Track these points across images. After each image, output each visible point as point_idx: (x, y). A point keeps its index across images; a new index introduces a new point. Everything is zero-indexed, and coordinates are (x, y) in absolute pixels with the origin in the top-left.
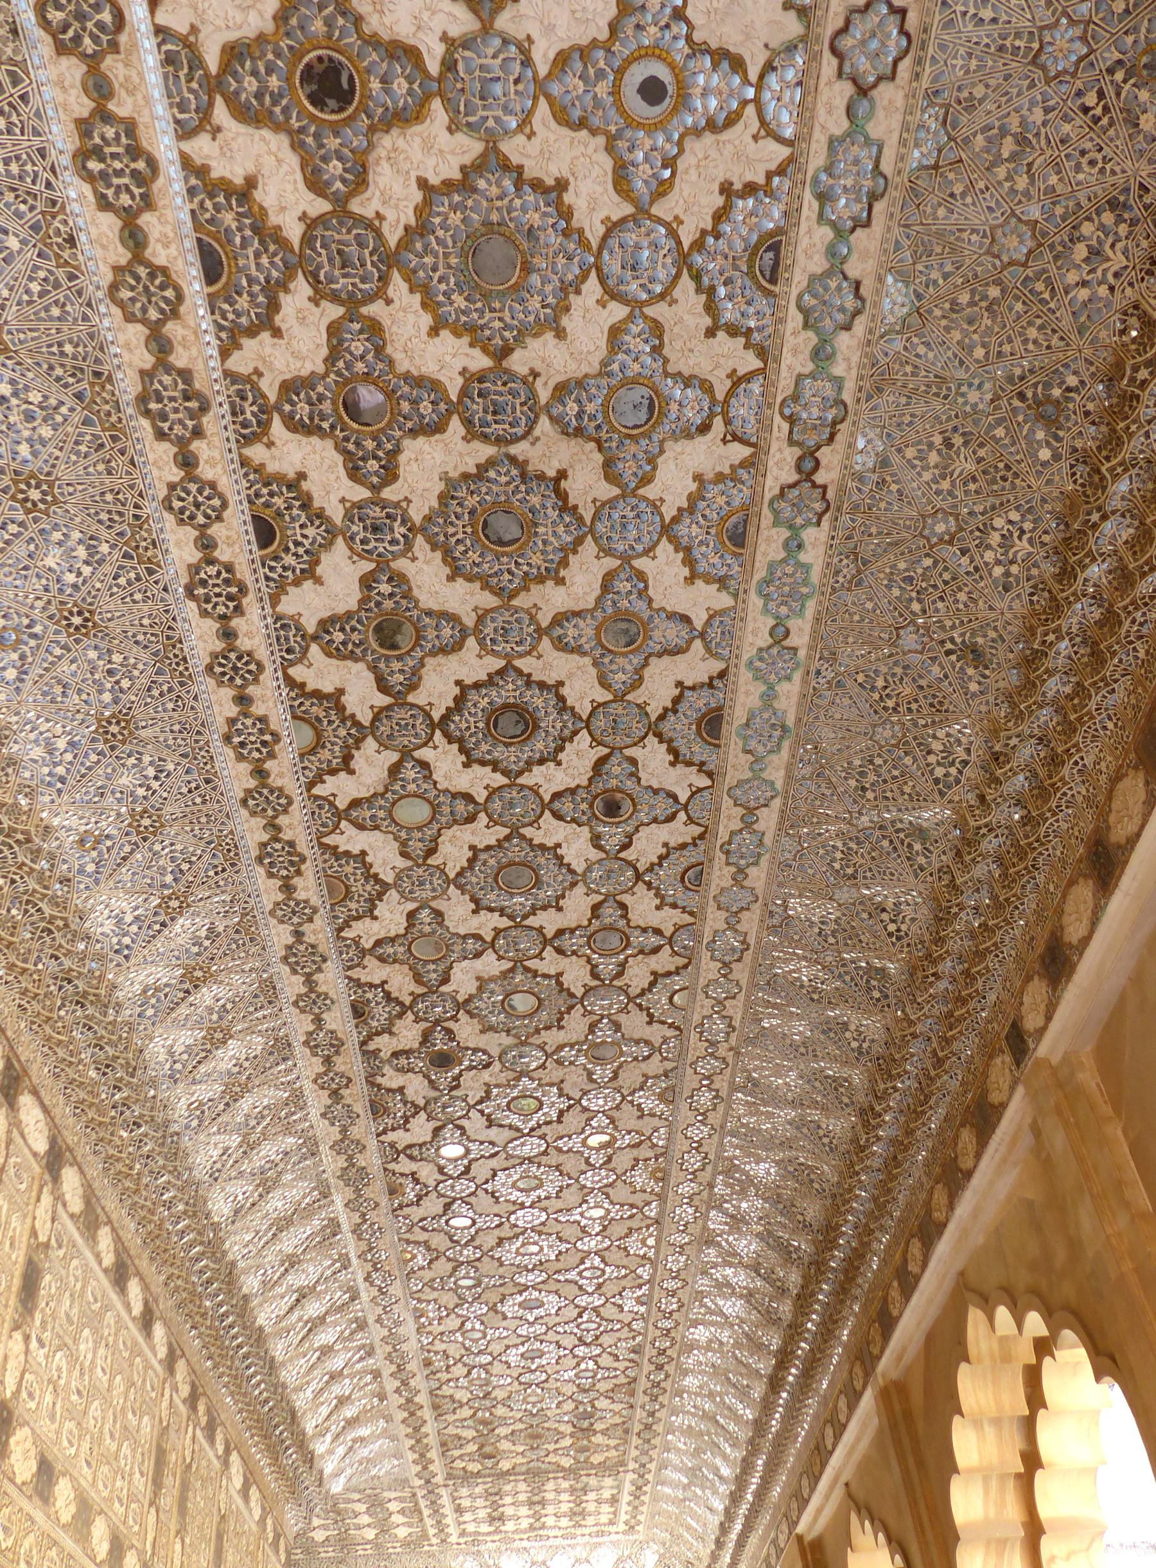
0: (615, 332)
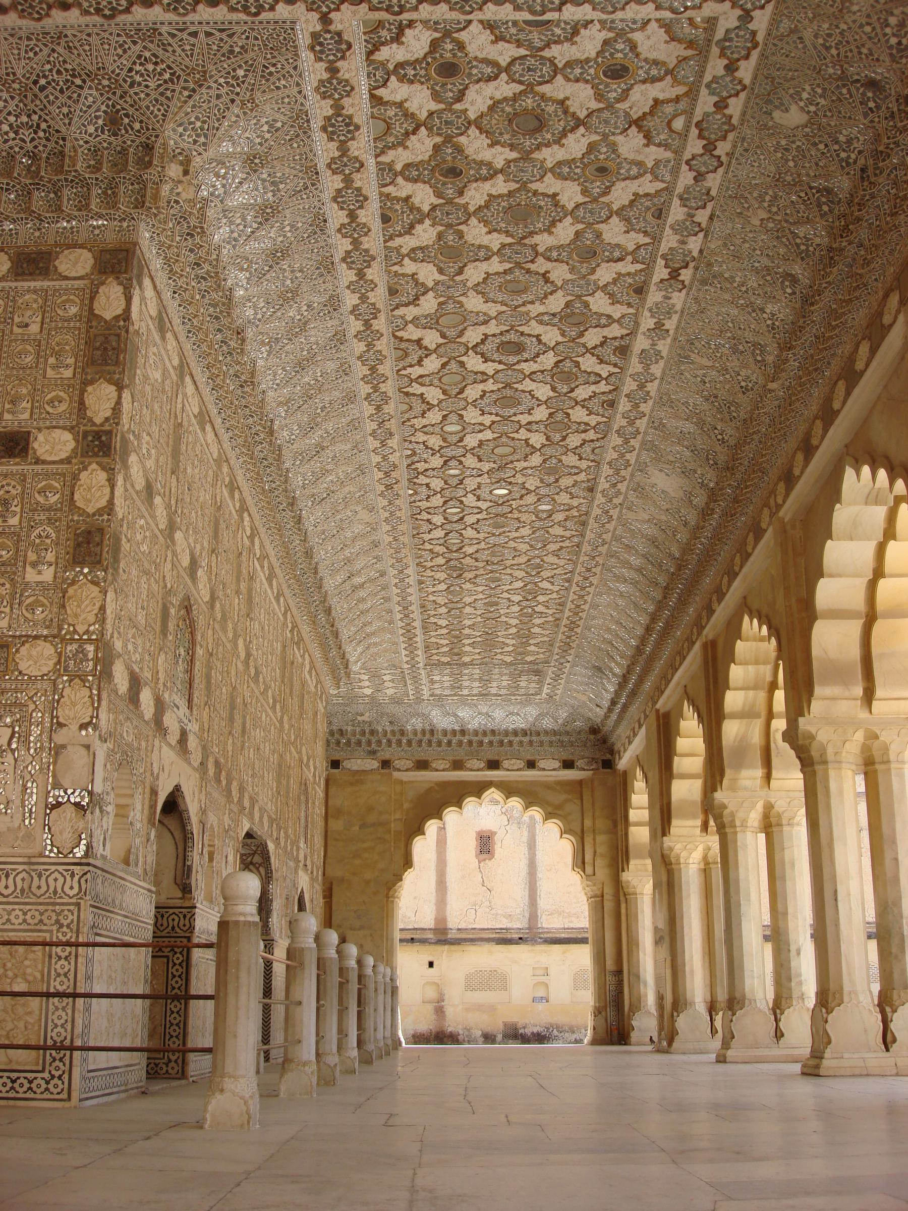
0: (577, 234)
